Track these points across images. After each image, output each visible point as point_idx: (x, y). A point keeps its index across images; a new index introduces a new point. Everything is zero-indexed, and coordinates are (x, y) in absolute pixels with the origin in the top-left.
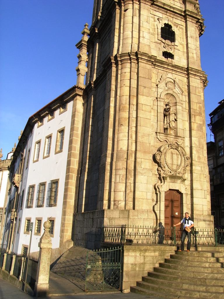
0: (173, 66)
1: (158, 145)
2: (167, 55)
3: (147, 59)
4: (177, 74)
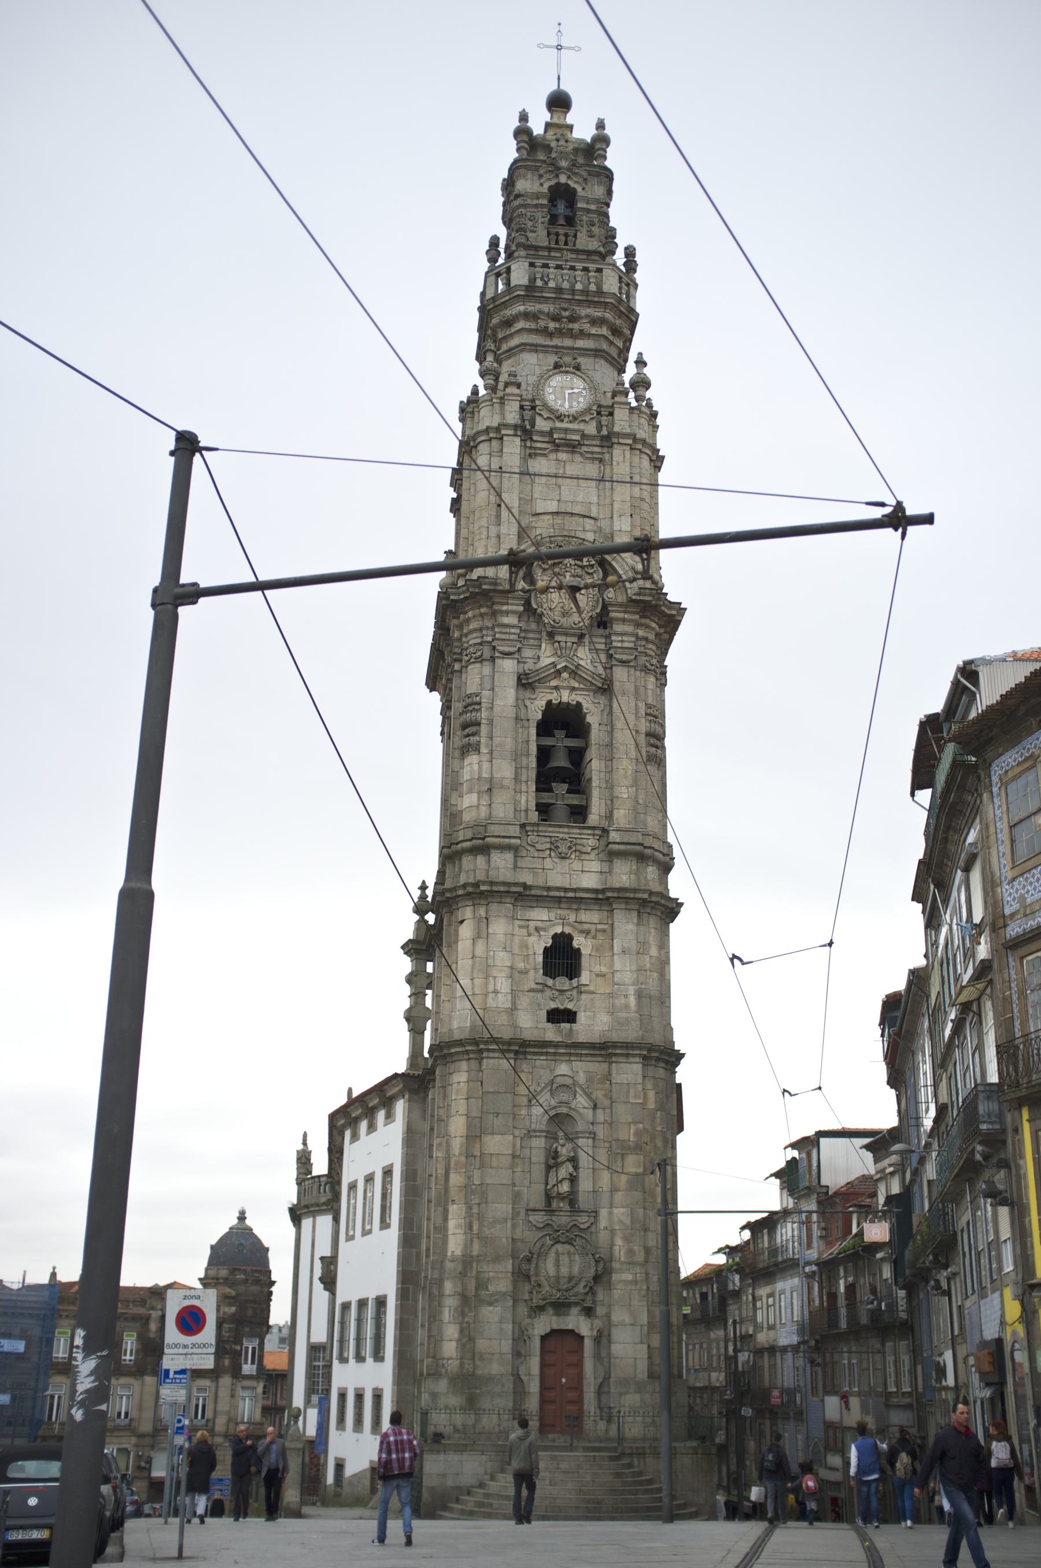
1: (532, 1236)
2: (561, 1016)
4: (584, 1058)
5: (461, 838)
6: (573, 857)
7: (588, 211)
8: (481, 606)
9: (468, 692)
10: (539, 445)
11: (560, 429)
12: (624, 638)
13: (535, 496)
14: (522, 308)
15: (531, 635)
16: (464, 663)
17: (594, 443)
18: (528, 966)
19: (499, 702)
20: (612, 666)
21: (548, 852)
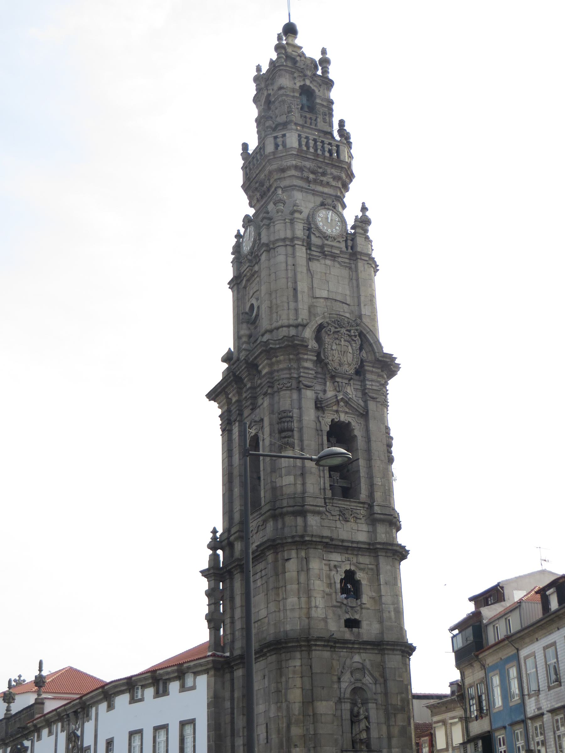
0: (360, 643)
2: (352, 624)
3: (323, 643)
4: (367, 651)
5: (285, 505)
7: (323, 105)
8: (289, 355)
9: (282, 409)
10: (314, 253)
11: (329, 245)
12: (373, 383)
13: (315, 286)
14: (294, 162)
15: (319, 376)
16: (275, 389)
17: (346, 256)
18: (331, 591)
19: (305, 418)
20: (367, 400)
21: (338, 517)
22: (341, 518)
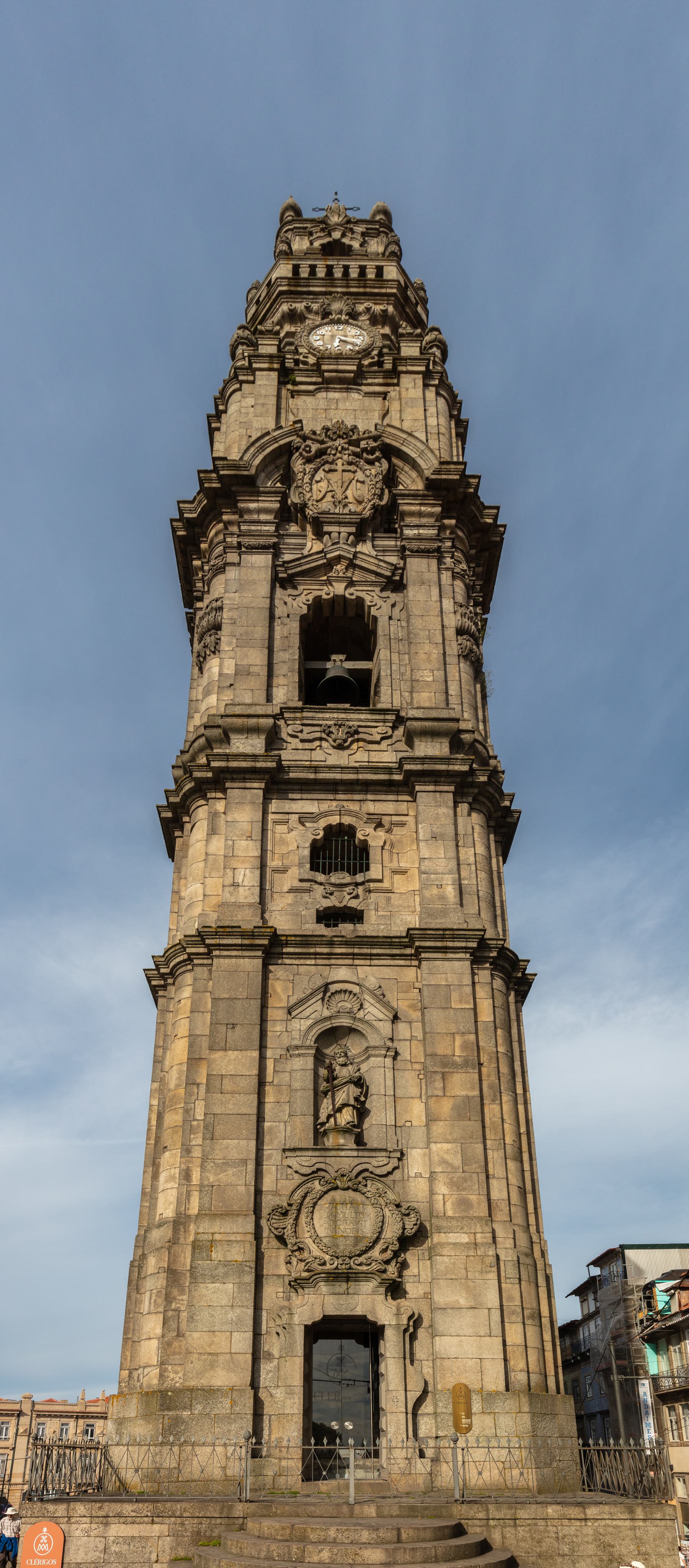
6: (355, 746)
17: (376, 381)
22: (324, 744)
